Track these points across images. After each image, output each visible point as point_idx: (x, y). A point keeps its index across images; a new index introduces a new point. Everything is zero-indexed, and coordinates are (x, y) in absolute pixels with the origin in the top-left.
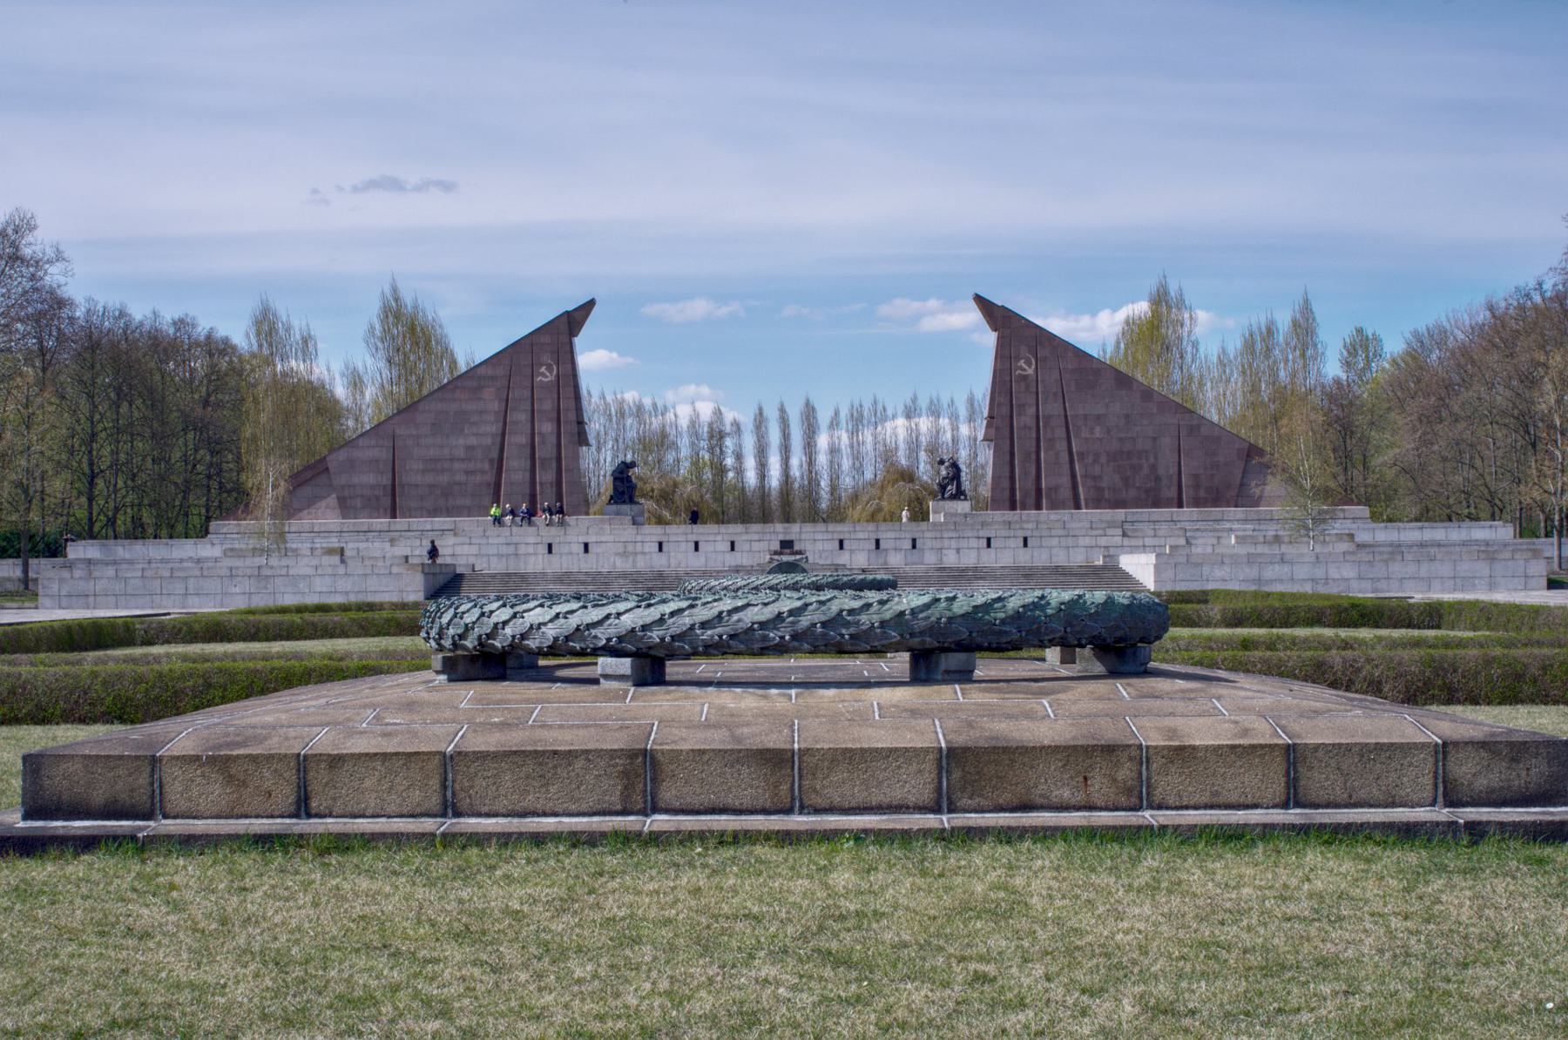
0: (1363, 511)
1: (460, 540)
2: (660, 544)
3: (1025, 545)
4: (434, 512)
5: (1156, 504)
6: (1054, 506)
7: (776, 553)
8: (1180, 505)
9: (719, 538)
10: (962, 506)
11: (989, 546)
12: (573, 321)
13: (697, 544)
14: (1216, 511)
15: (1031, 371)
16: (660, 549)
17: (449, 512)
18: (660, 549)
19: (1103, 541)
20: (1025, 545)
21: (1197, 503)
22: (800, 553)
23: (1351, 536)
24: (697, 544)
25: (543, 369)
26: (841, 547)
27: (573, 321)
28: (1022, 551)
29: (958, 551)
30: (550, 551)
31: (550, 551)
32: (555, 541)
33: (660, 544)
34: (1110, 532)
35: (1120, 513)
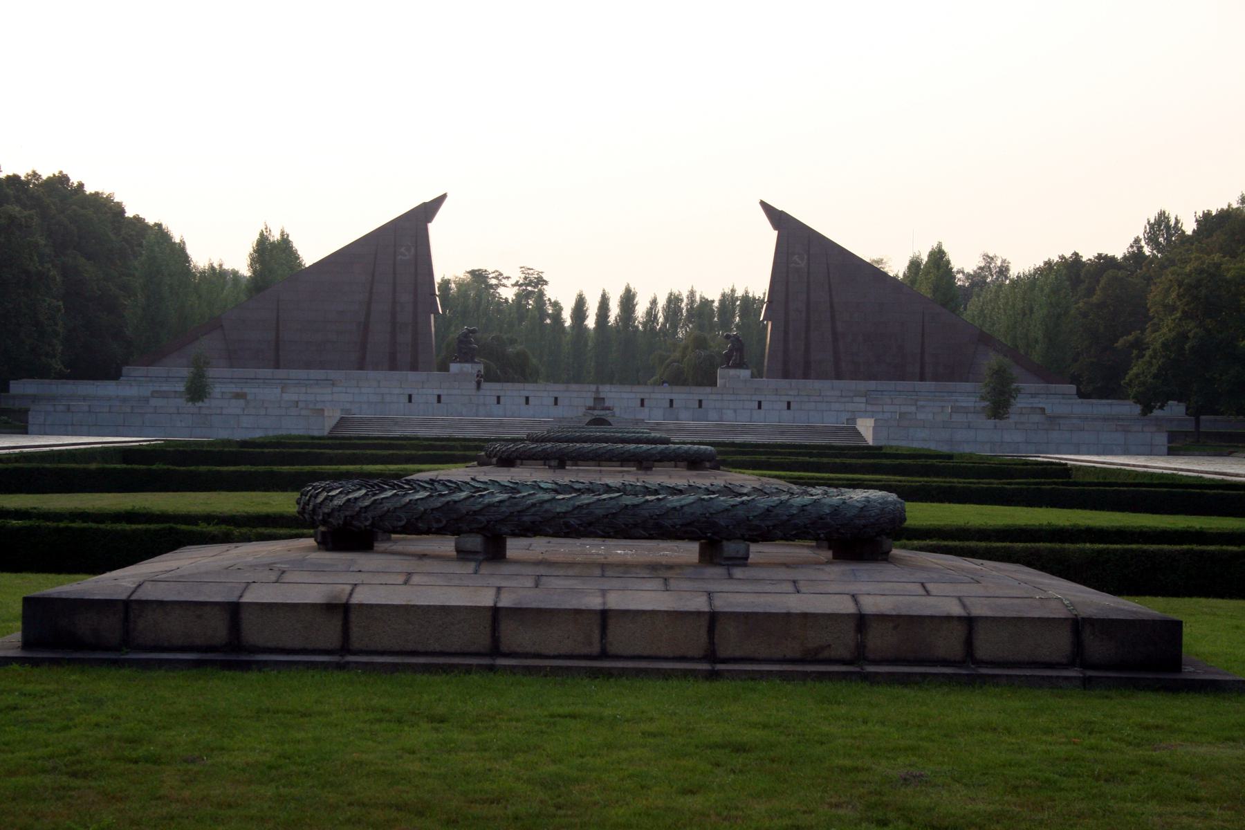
0: (1072, 388)
1: (335, 389)
2: (498, 398)
3: (789, 408)
4: (308, 365)
5: (902, 378)
6: (820, 377)
7: (590, 408)
8: (922, 379)
9: (545, 394)
10: (745, 373)
11: (760, 407)
12: (428, 210)
13: (527, 398)
14: (951, 385)
15: (803, 264)
16: (498, 402)
17: (322, 366)
18: (498, 402)
19: (850, 407)
20: (789, 408)
21: (936, 378)
22: (608, 409)
23: (1043, 409)
24: (527, 398)
25: (403, 250)
26: (642, 404)
27: (428, 210)
28: (786, 413)
29: (735, 411)
30: (410, 401)
31: (410, 401)
32: (414, 392)
33: (498, 398)
34: (856, 399)
35: (872, 385)
